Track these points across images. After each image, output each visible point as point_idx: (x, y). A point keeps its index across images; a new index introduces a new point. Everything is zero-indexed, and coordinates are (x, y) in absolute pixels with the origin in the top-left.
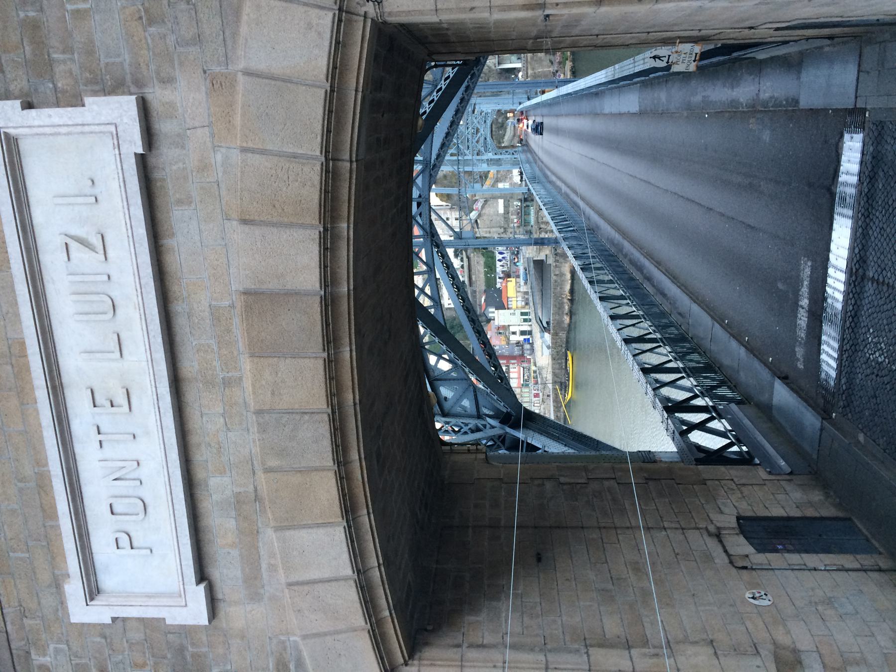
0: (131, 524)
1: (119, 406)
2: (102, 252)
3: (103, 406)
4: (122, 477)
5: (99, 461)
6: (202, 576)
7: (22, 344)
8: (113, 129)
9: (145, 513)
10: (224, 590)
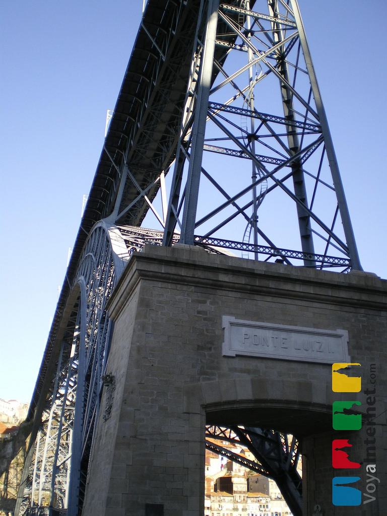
6: (237, 356)
7: (296, 325)
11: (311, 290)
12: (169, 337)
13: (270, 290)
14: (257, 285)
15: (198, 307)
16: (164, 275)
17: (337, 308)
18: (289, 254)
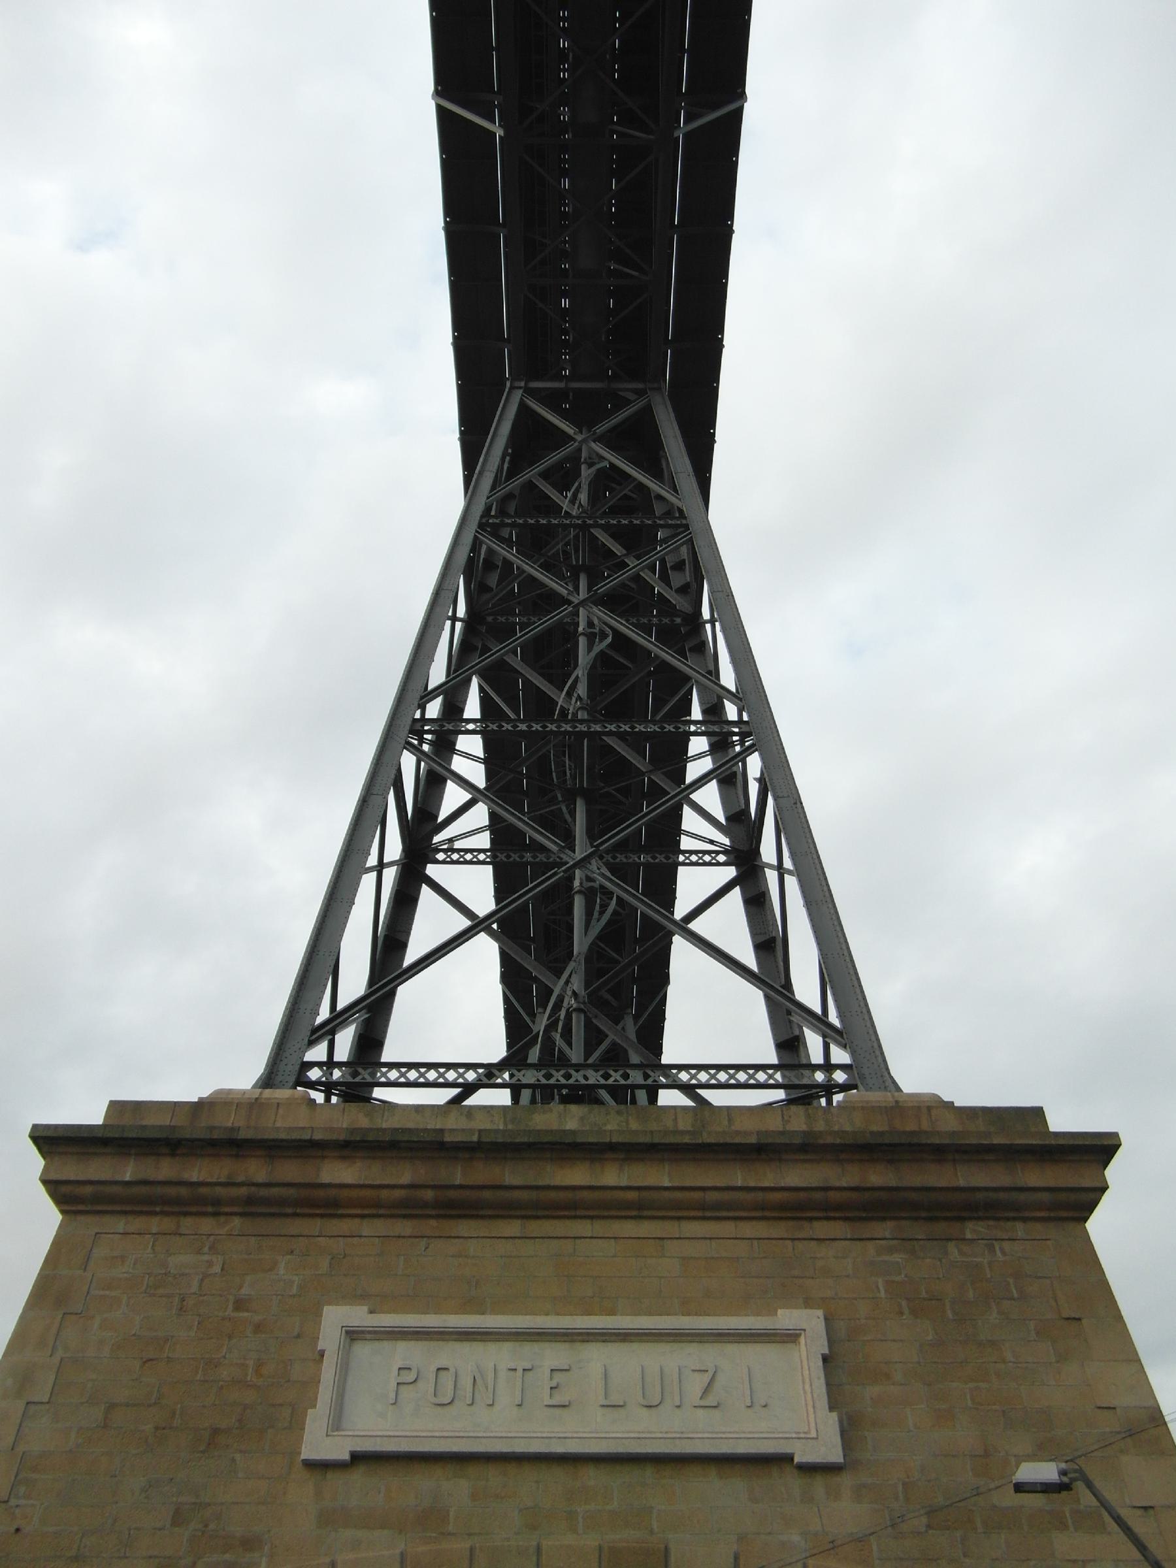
0: (426, 1385)
1: (551, 1395)
2: (703, 1403)
3: (551, 1379)
4: (476, 1387)
5: (495, 1365)
6: (358, 1458)
7: (612, 1312)
8: (813, 1434)
9: (435, 1404)
10: (335, 1480)
11: (657, 1175)
12: (112, 1406)
13: (508, 1195)
14: (458, 1182)
15: (241, 1287)
16: (135, 1190)
17: (779, 1229)
18: (703, 1077)
